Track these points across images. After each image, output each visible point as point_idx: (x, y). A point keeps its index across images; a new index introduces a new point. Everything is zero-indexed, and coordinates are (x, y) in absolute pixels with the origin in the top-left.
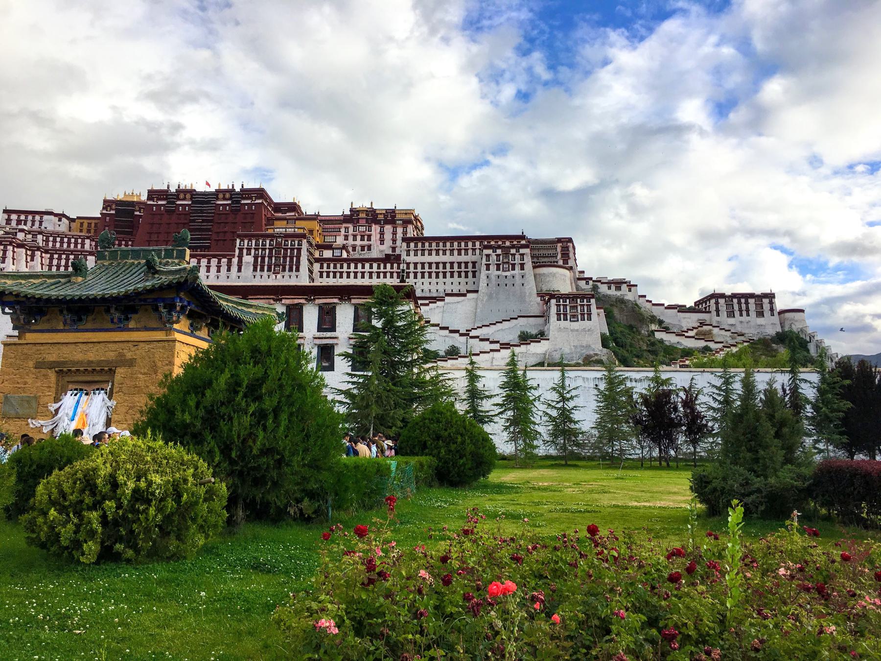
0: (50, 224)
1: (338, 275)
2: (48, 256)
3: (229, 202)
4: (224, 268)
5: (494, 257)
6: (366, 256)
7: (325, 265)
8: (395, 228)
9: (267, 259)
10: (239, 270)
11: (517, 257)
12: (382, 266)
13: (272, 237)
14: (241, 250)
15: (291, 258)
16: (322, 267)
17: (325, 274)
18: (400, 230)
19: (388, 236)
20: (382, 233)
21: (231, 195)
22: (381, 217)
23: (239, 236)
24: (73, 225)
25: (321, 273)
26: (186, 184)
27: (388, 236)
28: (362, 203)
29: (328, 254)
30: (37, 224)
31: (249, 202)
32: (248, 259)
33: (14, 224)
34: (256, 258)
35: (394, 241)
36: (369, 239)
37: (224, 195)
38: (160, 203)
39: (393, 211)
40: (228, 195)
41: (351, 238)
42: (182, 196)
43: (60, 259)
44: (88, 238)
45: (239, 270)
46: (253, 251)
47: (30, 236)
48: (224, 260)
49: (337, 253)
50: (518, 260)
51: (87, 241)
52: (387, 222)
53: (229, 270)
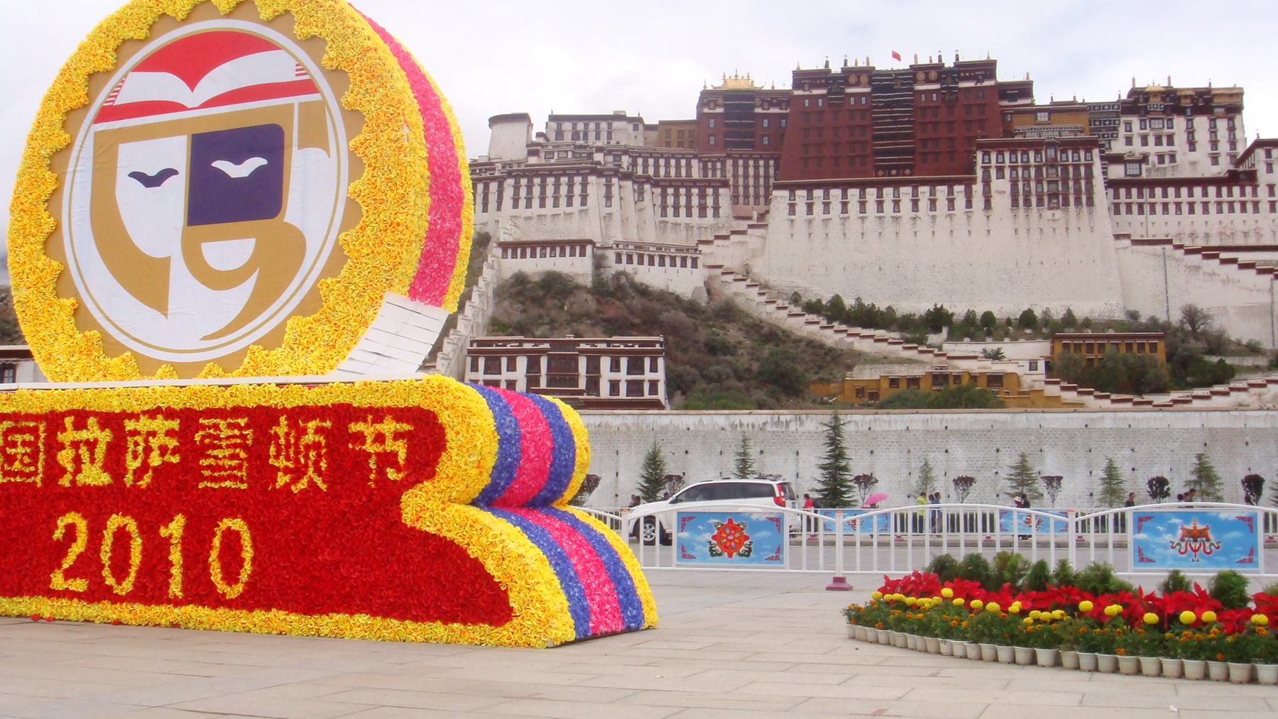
0: (625, 137)
1: (1147, 208)
2: (658, 191)
3: (937, 86)
4: (960, 201)
6: (1169, 175)
7: (1122, 191)
8: (1213, 121)
9: (1033, 184)
10: (988, 204)
12: (1224, 190)
13: (1037, 146)
14: (986, 170)
15: (1077, 181)
16: (1117, 196)
17: (1123, 209)
18: (1222, 125)
19: (1202, 135)
20: (1190, 132)
21: (940, 74)
22: (1186, 103)
23: (980, 146)
24: (653, 135)
25: (1117, 206)
26: (858, 60)
27: (1202, 135)
28: (1152, 79)
30: (604, 135)
31: (971, 84)
32: (1001, 186)
33: (568, 138)
34: (1014, 183)
35: (1214, 144)
37: (927, 74)
38: (815, 92)
39: (1208, 91)
40: (933, 75)
41: (1137, 141)
42: (853, 79)
43: (677, 195)
44: (695, 157)
45: (988, 204)
46: (1007, 172)
47: (610, 158)
49: (1133, 169)
51: (695, 162)
52: (1198, 111)
53: (969, 204)
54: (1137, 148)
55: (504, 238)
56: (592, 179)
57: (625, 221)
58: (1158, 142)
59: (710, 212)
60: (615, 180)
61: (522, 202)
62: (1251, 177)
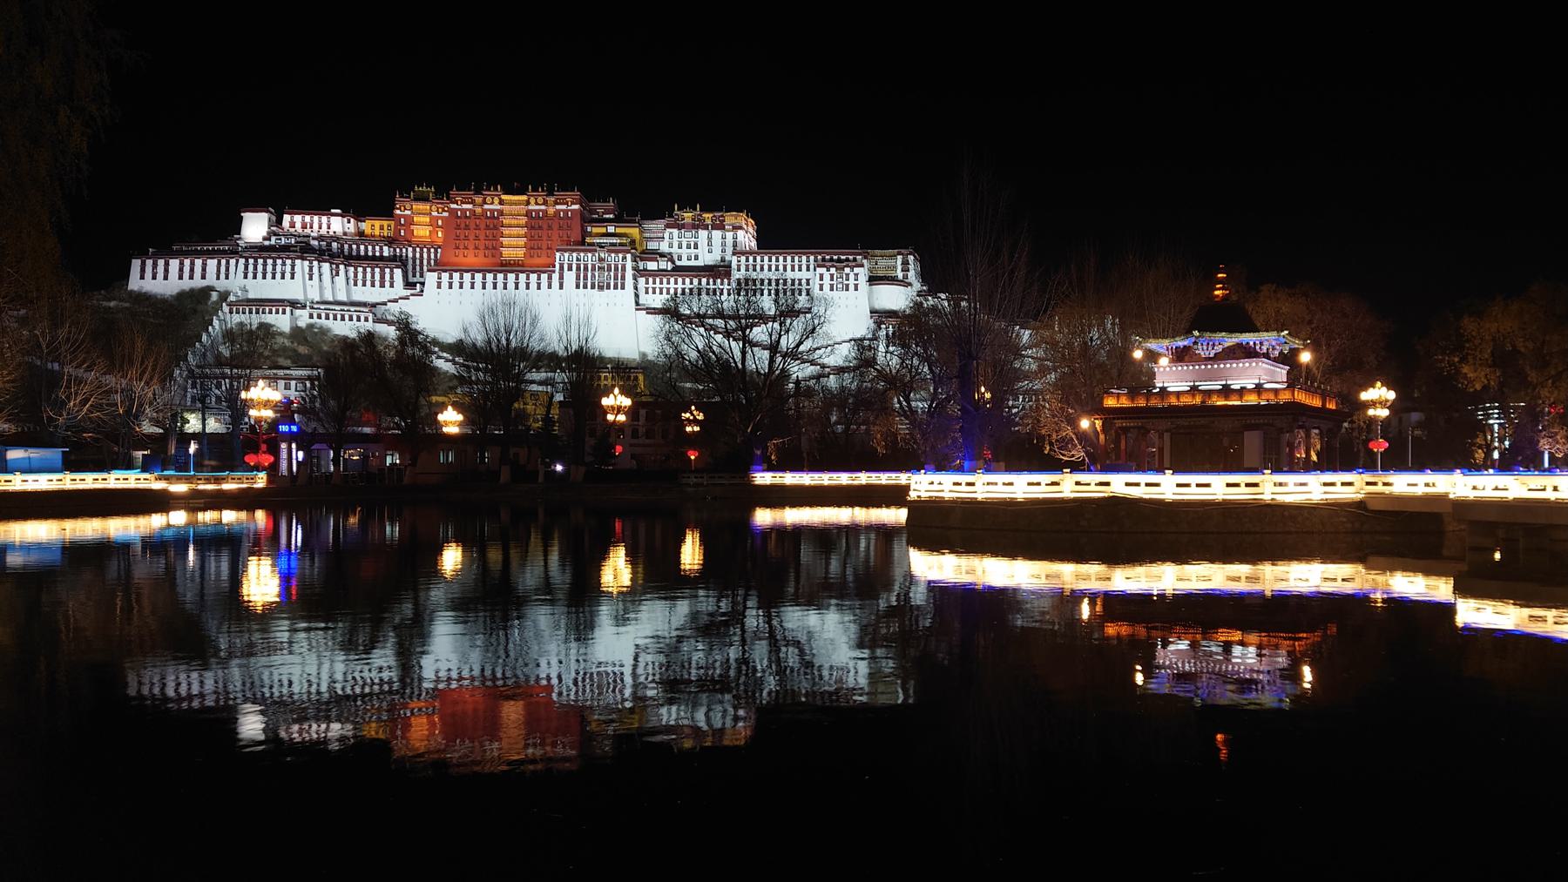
5: (827, 277)
10: (561, 287)
11: (852, 276)
15: (616, 278)
20: (710, 239)
29: (652, 266)
30: (324, 226)
32: (570, 277)
33: (298, 226)
36: (696, 247)
40: (540, 200)
42: (489, 199)
45: (561, 287)
48: (544, 277)
50: (852, 282)
51: (386, 249)
53: (550, 287)
54: (675, 250)
55: (232, 298)
56: (298, 262)
57: (321, 288)
58: (689, 247)
59: (387, 284)
60: (315, 263)
61: (250, 275)
62: (728, 274)
